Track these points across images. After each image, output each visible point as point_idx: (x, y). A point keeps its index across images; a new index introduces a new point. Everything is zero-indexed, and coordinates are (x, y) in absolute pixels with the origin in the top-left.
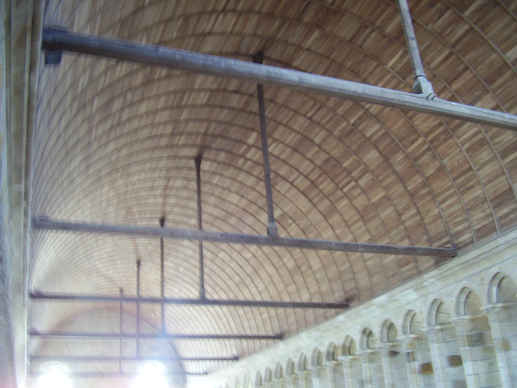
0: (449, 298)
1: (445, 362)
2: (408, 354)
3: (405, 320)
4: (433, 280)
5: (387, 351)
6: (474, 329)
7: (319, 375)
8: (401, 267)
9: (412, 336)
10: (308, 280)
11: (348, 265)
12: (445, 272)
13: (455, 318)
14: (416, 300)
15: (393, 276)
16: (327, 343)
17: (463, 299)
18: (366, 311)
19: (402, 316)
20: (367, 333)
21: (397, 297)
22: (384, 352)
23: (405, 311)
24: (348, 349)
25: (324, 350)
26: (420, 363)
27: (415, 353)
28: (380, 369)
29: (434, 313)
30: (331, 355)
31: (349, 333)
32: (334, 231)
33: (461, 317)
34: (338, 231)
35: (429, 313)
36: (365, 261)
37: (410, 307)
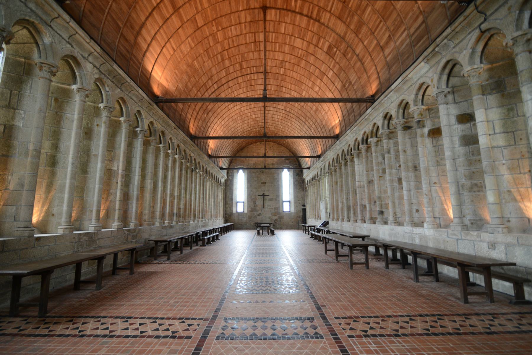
0: (463, 52)
1: (453, 120)
2: (419, 121)
3: (417, 94)
4: (446, 40)
5: (403, 126)
6: (491, 77)
7: (358, 156)
8: (415, 46)
9: (423, 107)
10: (350, 93)
11: (374, 68)
12: (460, 24)
13: (469, 68)
14: (427, 72)
15: (408, 58)
16: (362, 133)
17: (480, 48)
18: (386, 98)
19: (414, 92)
20: (388, 117)
21: (410, 76)
22: (399, 127)
23: (417, 86)
24: (375, 133)
25: (360, 139)
26: (430, 128)
27: (425, 121)
28: (396, 144)
29: (445, 77)
30: (365, 141)
31: (375, 121)
32: (363, 43)
33: (476, 66)
34: (365, 43)
35: (440, 78)
36: (386, 58)
37: (421, 81)
